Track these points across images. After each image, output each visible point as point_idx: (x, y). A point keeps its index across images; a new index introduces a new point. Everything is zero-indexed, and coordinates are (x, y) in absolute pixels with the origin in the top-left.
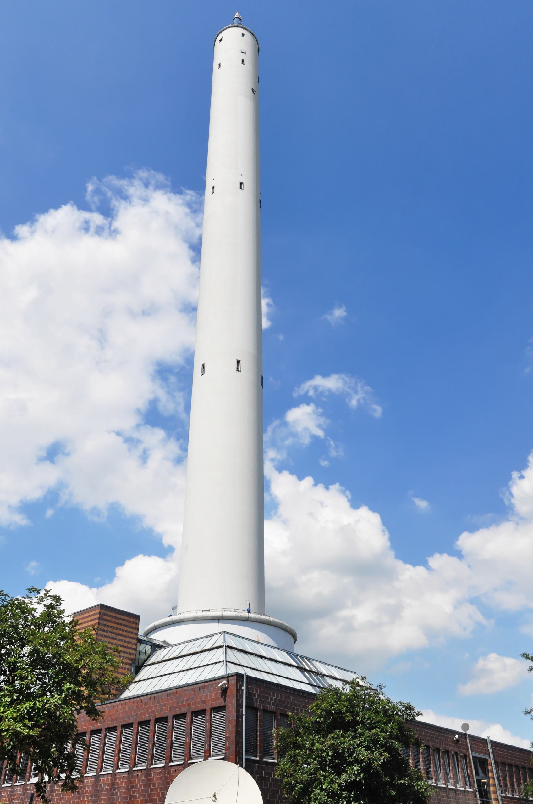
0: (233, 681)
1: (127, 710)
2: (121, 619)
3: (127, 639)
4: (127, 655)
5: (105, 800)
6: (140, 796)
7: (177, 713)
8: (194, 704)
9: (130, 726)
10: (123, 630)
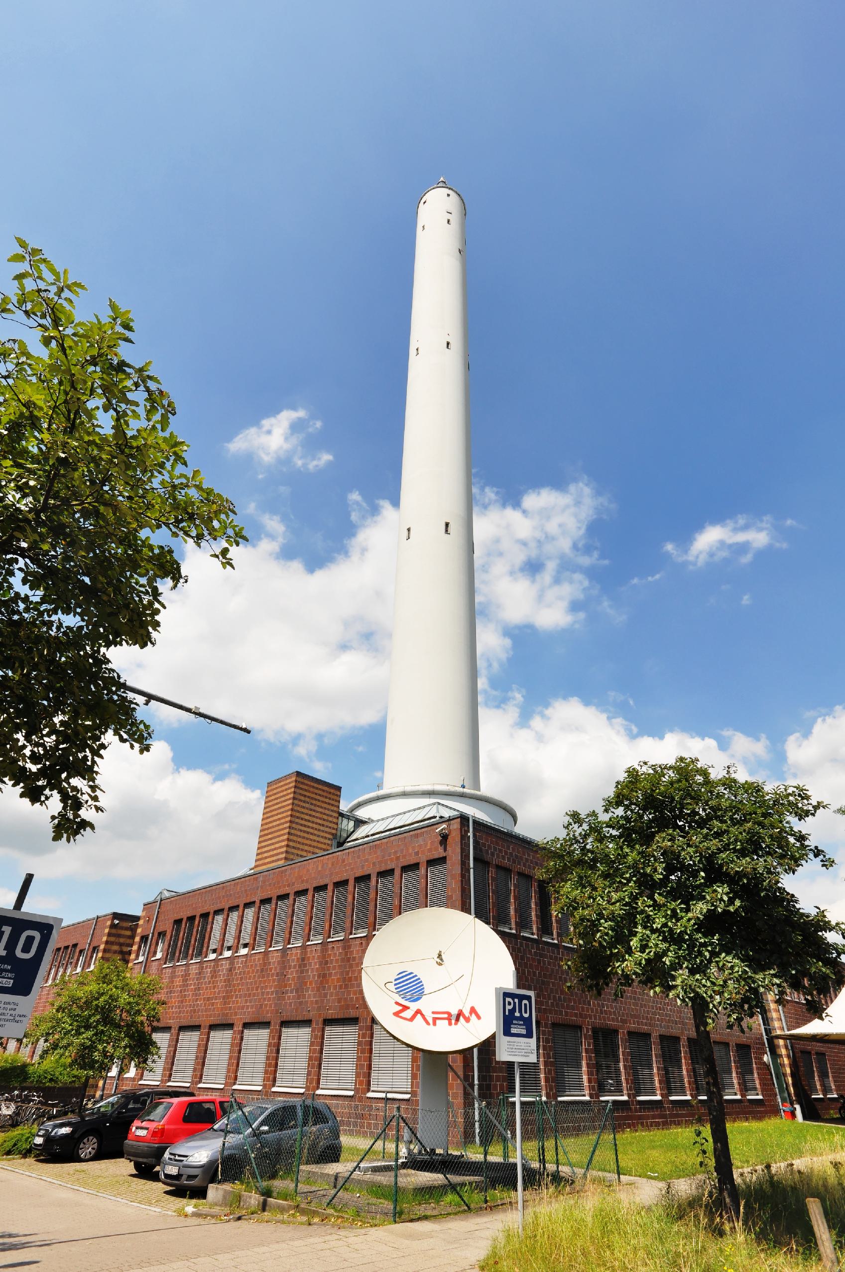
0: (456, 825)
1: (320, 869)
2: (320, 789)
3: (327, 812)
5: (293, 979)
8: (404, 857)
9: (323, 888)
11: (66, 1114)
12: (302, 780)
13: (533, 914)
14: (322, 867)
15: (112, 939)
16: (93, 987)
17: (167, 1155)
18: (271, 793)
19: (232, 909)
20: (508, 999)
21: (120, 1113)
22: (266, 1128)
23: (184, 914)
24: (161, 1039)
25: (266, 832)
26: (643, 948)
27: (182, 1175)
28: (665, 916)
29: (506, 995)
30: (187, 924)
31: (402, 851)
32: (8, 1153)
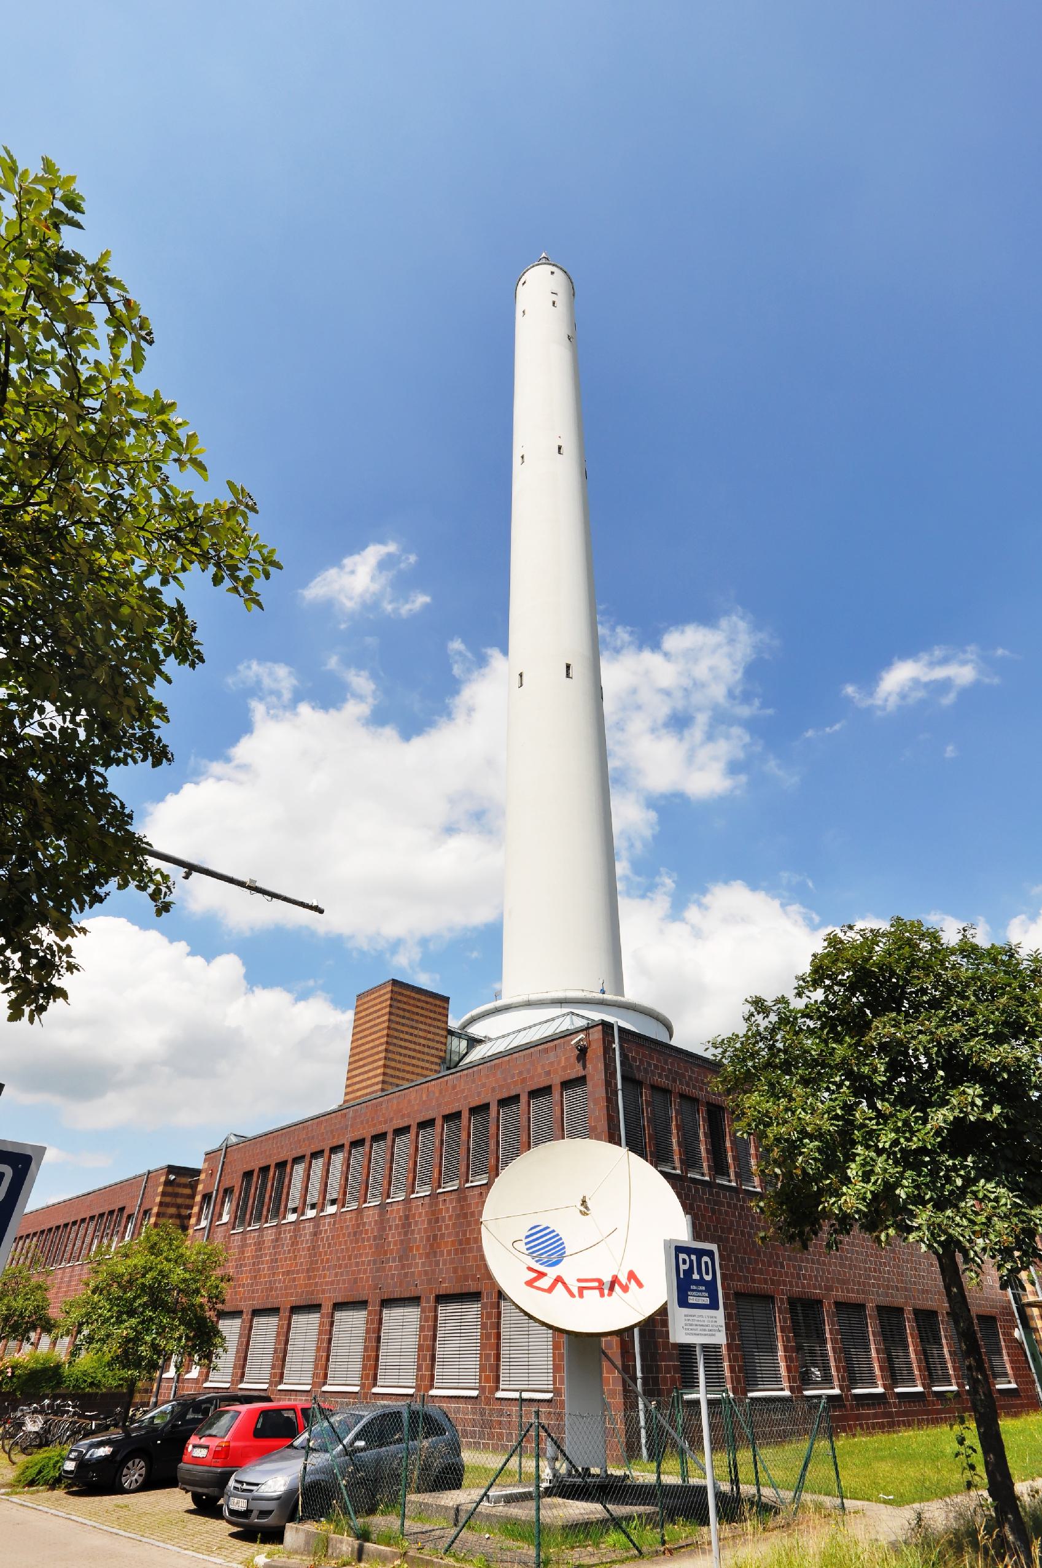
0: (597, 1034)
4: (433, 1052)
5: (395, 1243)
6: (450, 1235)
7: (505, 1095)
8: (532, 1078)
9: (430, 1123)
10: (426, 1017)
11: (107, 1428)
12: (400, 990)
13: (703, 1148)
14: (428, 1096)
15: (168, 1199)
16: (138, 1261)
17: (232, 1483)
18: (361, 1008)
19: (315, 1155)
20: (682, 1256)
21: (175, 1426)
22: (361, 1444)
23: (255, 1165)
24: (230, 1329)
25: (357, 1057)
26: (866, 1177)
27: (251, 1511)
28: (897, 1130)
29: (679, 1249)
30: (259, 1177)
31: (528, 1071)
32: (32, 1483)
